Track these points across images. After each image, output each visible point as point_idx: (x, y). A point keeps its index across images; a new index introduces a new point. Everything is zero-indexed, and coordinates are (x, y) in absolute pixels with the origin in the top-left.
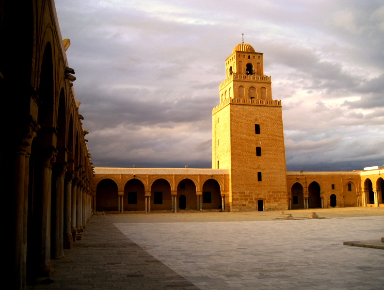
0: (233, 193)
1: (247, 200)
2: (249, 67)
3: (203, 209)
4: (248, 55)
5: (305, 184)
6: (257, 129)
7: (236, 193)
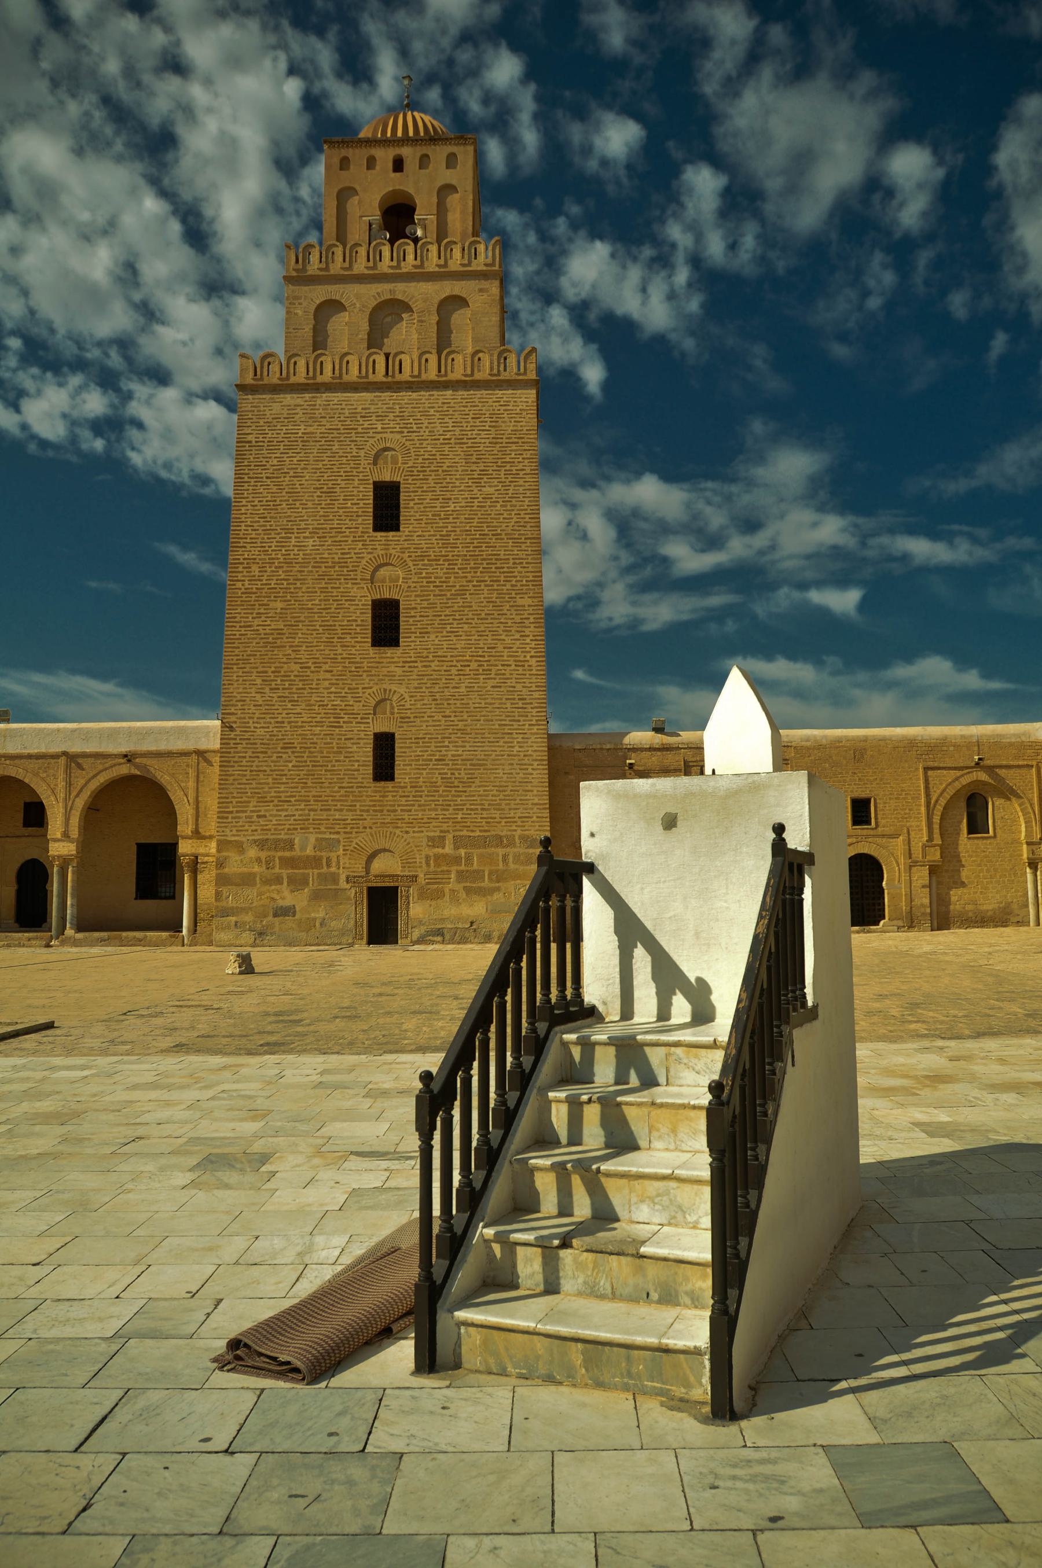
0: (222, 845)
1: (304, 882)
3: (80, 928)
6: (387, 508)
7: (240, 847)
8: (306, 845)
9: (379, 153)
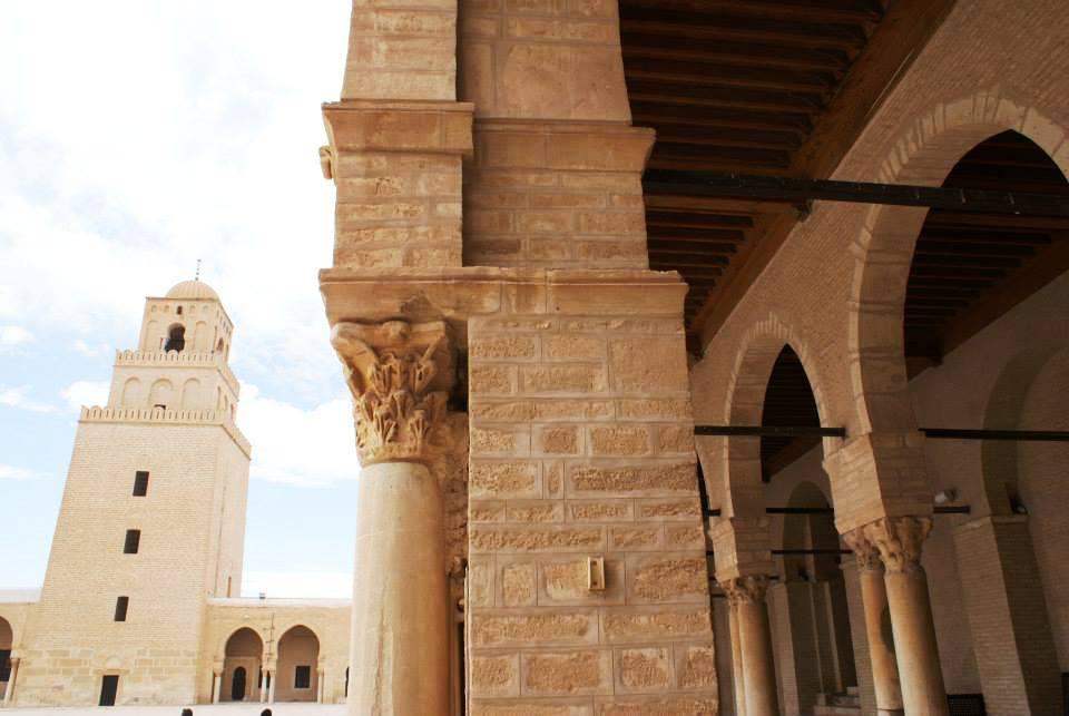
2: (176, 340)
4: (178, 304)
5: (269, 632)
6: (141, 484)
8: (75, 652)
9: (171, 304)
